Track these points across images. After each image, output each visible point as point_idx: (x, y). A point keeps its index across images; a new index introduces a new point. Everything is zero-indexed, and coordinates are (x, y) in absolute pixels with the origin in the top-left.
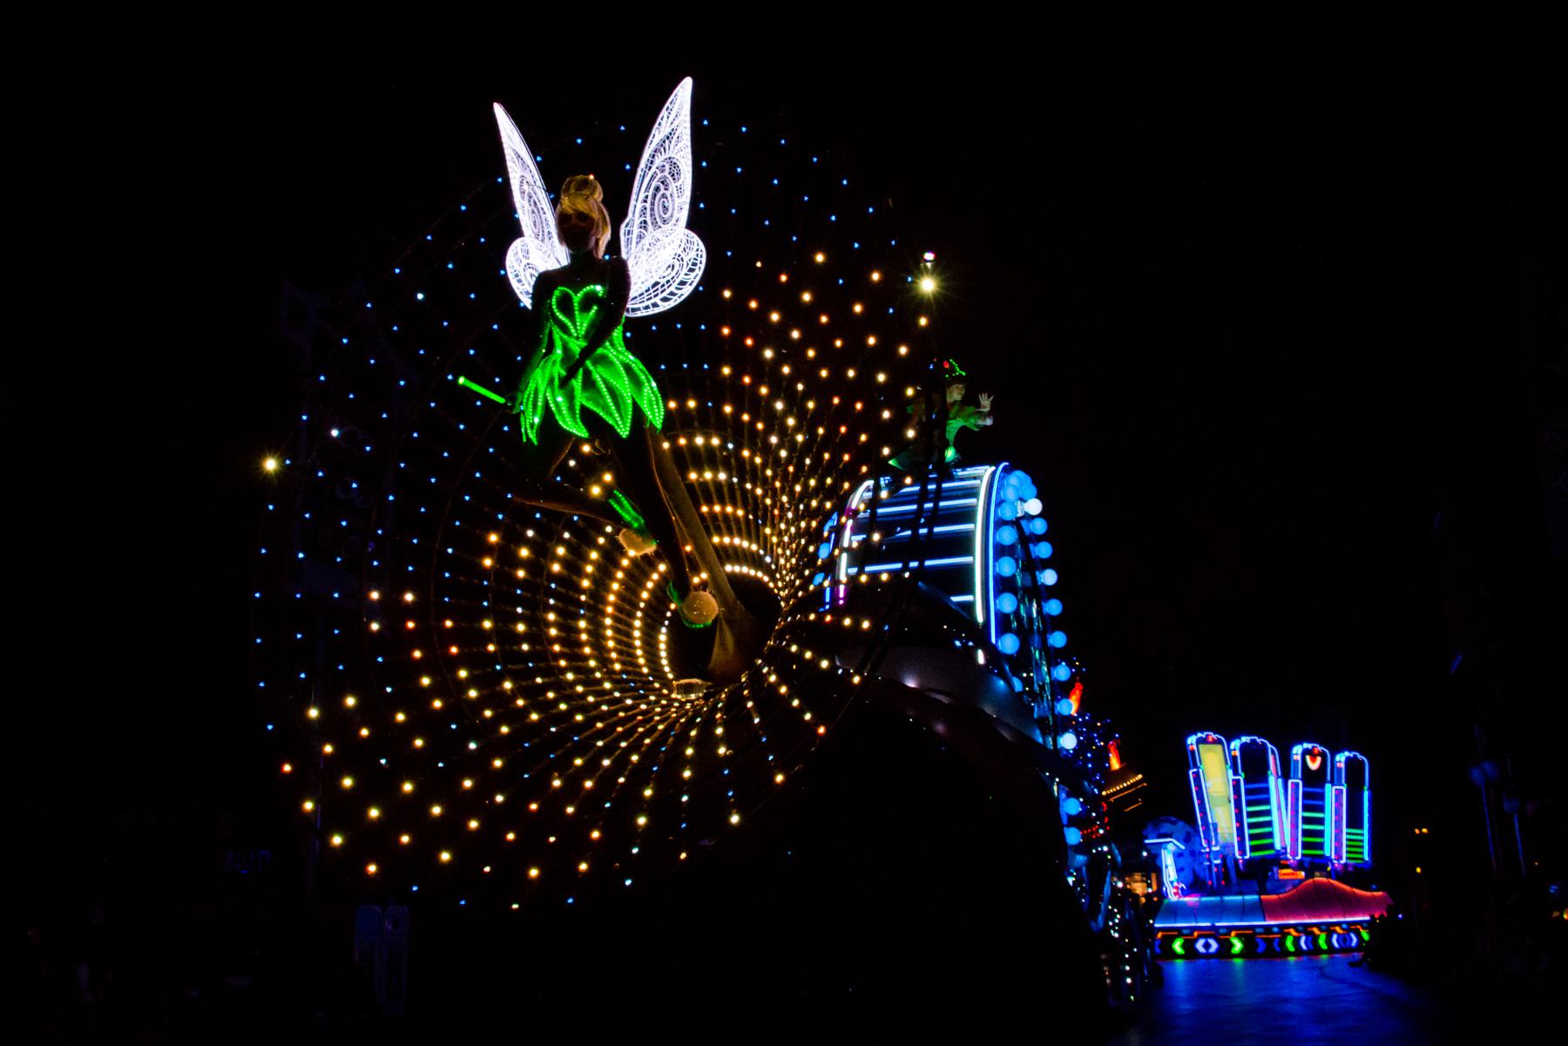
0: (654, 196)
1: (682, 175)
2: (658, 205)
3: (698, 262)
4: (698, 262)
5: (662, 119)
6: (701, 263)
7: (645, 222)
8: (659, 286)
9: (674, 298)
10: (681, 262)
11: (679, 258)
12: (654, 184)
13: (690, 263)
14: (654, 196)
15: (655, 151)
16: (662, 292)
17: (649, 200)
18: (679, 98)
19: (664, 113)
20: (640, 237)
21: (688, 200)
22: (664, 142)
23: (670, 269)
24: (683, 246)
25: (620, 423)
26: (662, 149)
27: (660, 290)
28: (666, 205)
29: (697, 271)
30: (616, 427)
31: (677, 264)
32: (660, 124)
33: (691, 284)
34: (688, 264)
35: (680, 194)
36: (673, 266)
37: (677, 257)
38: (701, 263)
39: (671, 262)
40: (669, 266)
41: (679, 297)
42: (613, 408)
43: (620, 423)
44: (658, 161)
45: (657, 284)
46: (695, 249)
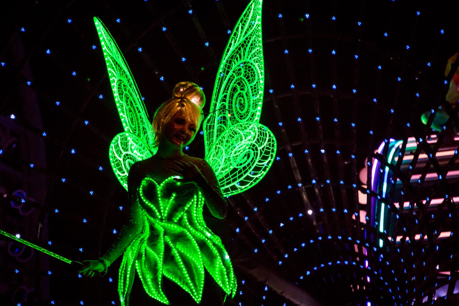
25: (194, 291)
43: (194, 291)
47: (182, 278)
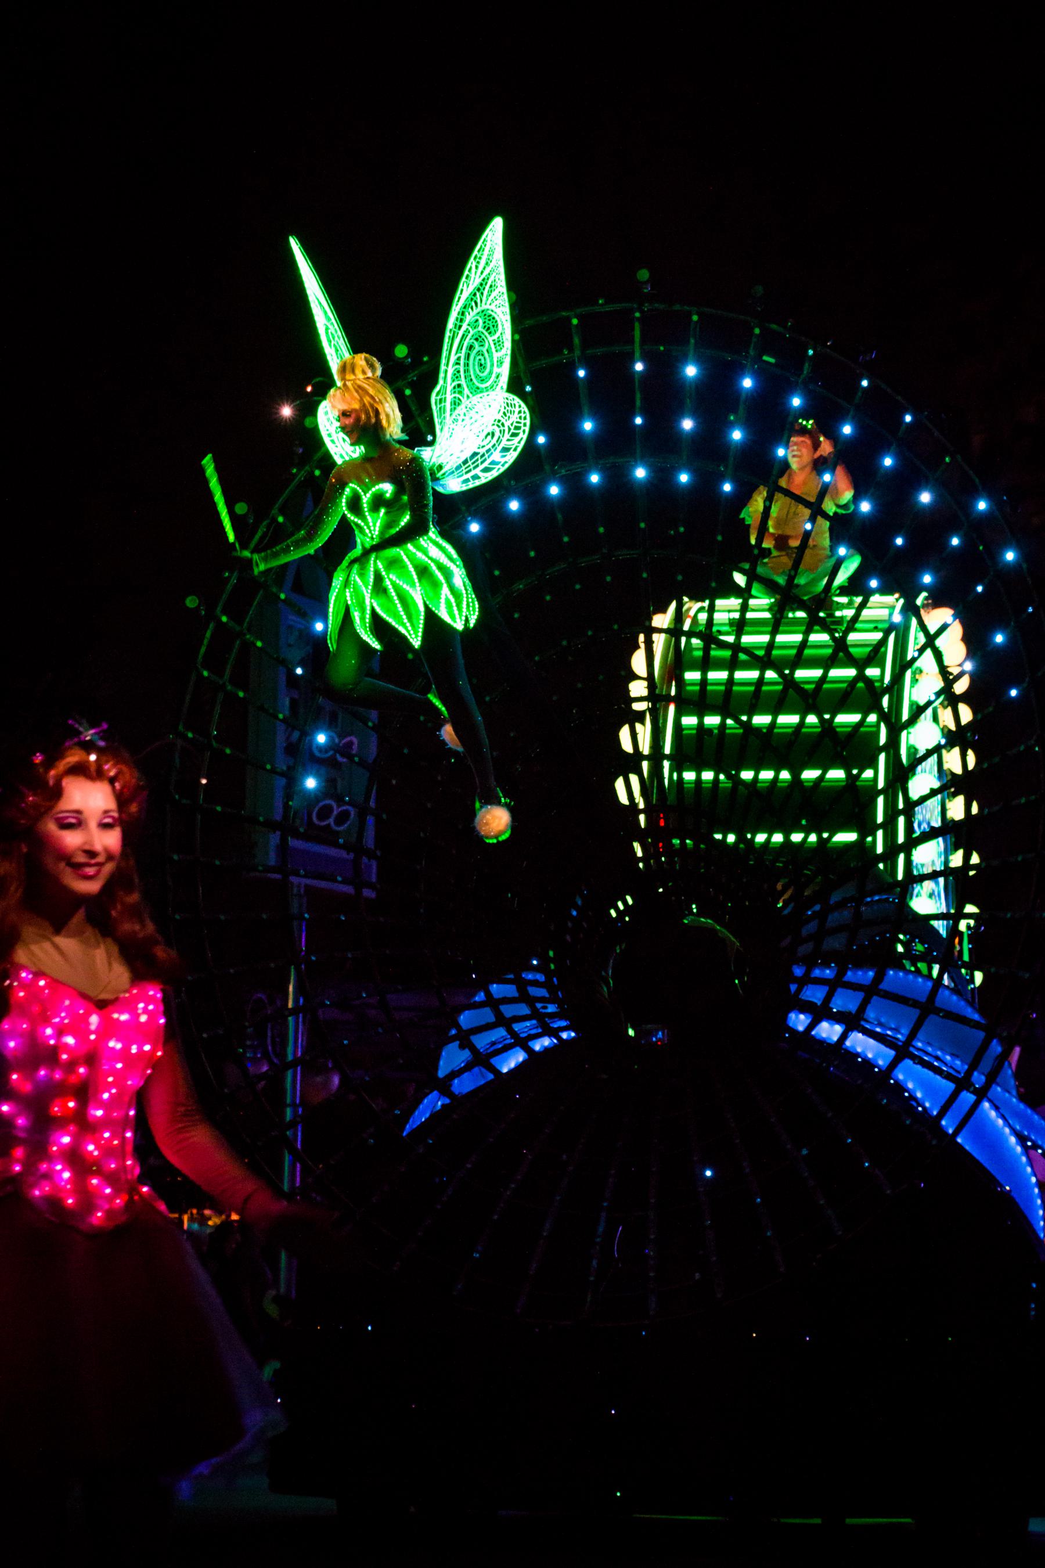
0: (468, 356)
1: (500, 327)
2: (474, 365)
3: (522, 425)
4: (522, 425)
5: (470, 270)
6: (525, 425)
7: (459, 386)
8: (479, 456)
9: (497, 467)
10: (502, 428)
11: (499, 423)
12: (466, 344)
13: (512, 428)
14: (468, 356)
15: (465, 308)
16: (482, 463)
17: (462, 362)
18: (488, 244)
19: (471, 263)
20: (456, 403)
21: (509, 352)
22: (475, 295)
23: (489, 437)
24: (503, 410)
25: (412, 632)
26: (473, 304)
27: (480, 461)
28: (483, 362)
29: (521, 435)
30: (409, 637)
31: (497, 430)
32: (467, 277)
33: (515, 450)
34: (509, 429)
35: (498, 348)
36: (493, 435)
37: (496, 423)
38: (525, 425)
39: (490, 430)
40: (489, 434)
41: (503, 465)
42: (404, 617)
43: (412, 632)
44: (469, 318)
45: (475, 454)
46: (517, 412)
47: (396, 616)
